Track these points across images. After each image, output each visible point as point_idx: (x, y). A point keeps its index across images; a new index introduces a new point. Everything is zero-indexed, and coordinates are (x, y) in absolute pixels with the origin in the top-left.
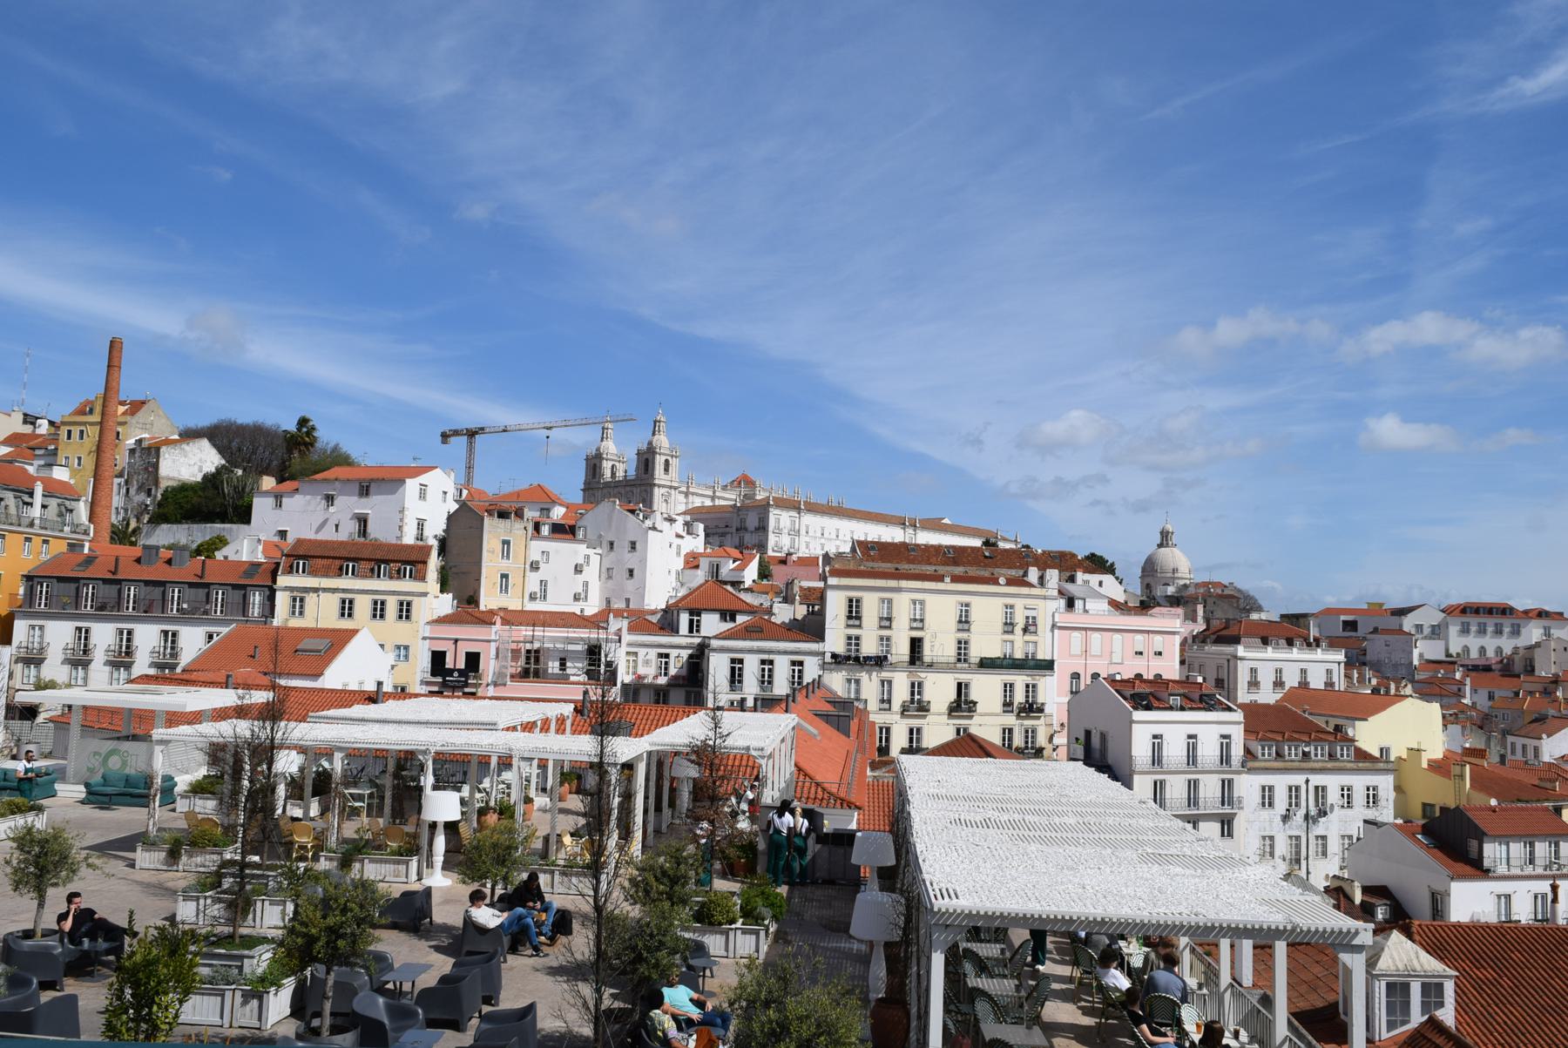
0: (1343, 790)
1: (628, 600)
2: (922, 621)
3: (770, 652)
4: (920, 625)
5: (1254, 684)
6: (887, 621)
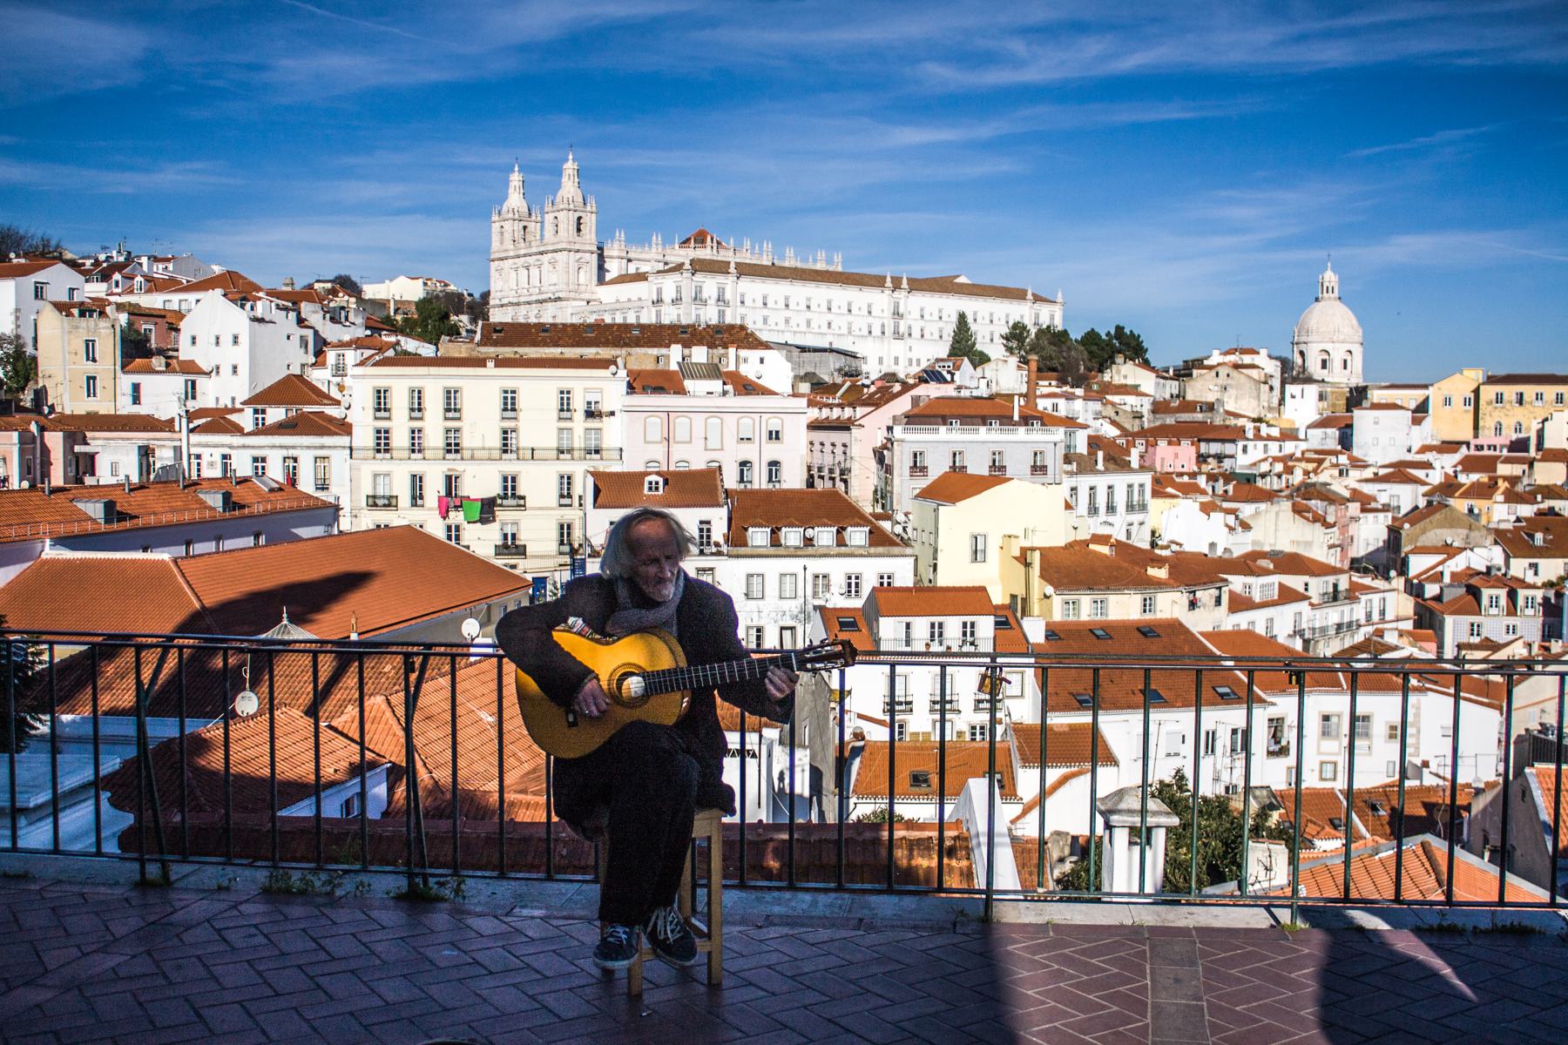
0: (850, 578)
1: (233, 399)
2: (459, 410)
3: (293, 447)
5: (918, 468)
6: (417, 408)
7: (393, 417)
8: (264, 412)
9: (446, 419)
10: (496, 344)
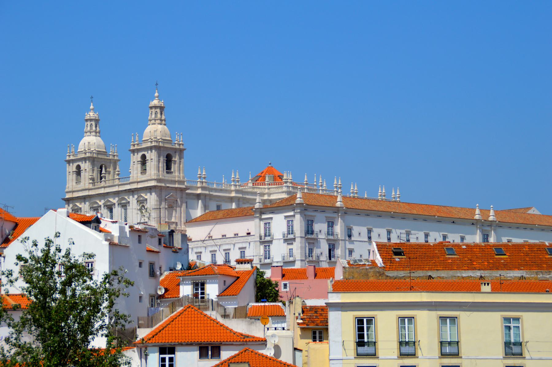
4: (454, 350)
7: (380, 353)
8: (172, 351)
9: (443, 355)
10: (401, 266)
